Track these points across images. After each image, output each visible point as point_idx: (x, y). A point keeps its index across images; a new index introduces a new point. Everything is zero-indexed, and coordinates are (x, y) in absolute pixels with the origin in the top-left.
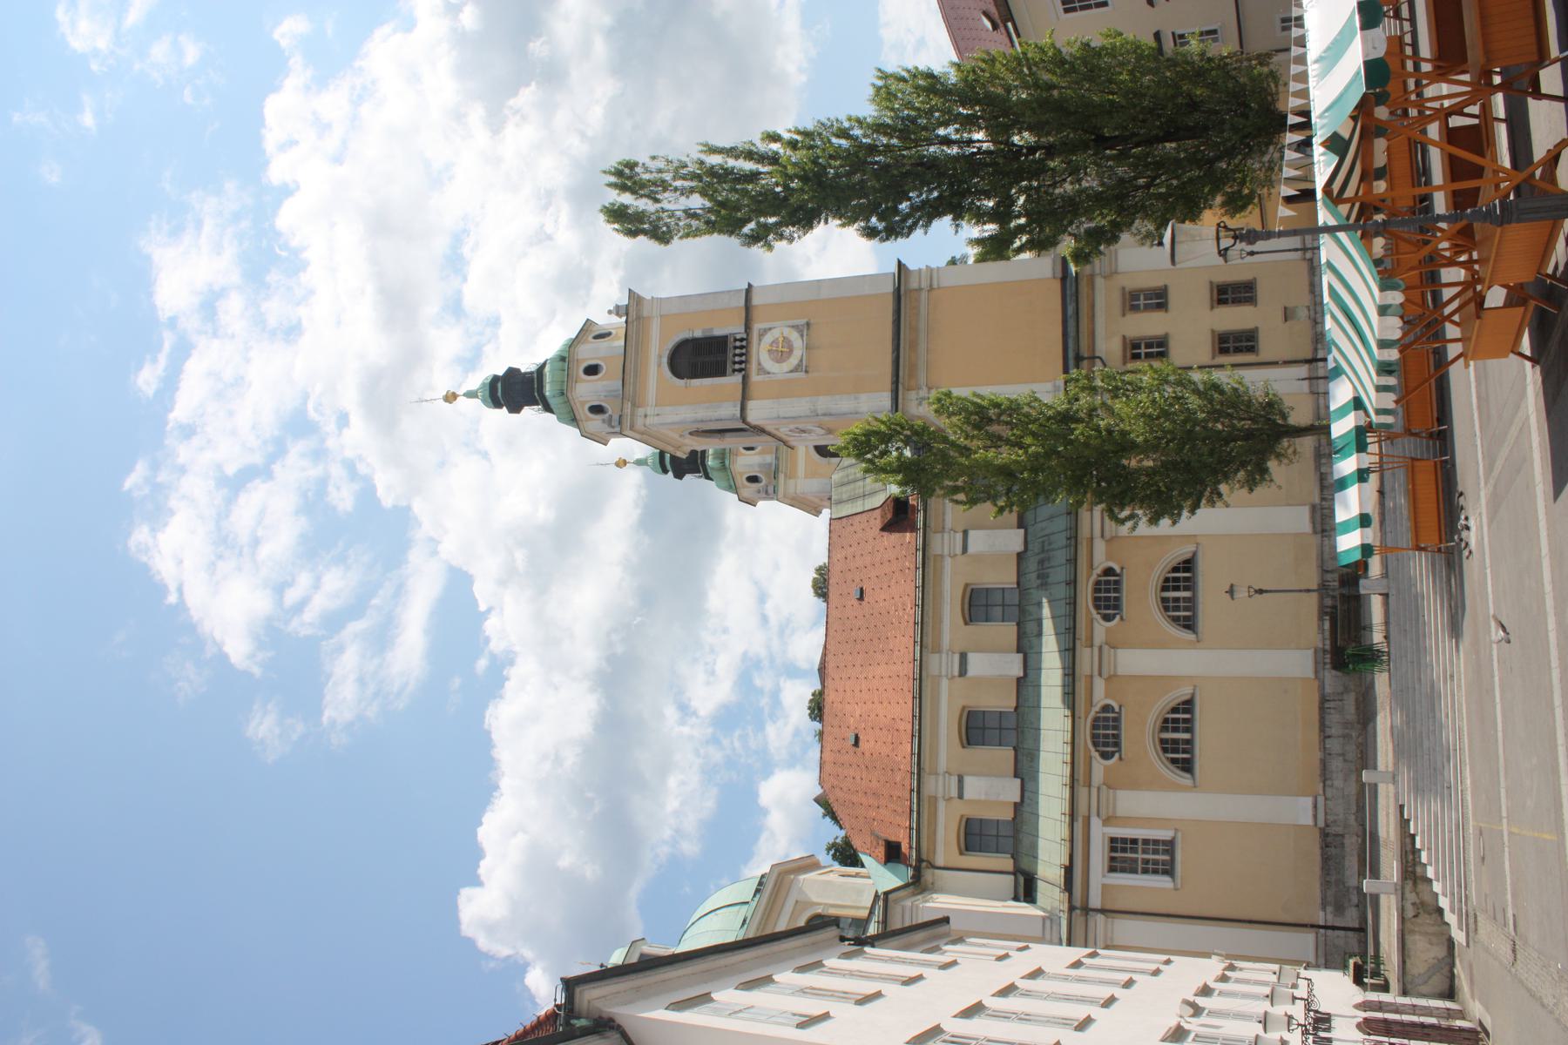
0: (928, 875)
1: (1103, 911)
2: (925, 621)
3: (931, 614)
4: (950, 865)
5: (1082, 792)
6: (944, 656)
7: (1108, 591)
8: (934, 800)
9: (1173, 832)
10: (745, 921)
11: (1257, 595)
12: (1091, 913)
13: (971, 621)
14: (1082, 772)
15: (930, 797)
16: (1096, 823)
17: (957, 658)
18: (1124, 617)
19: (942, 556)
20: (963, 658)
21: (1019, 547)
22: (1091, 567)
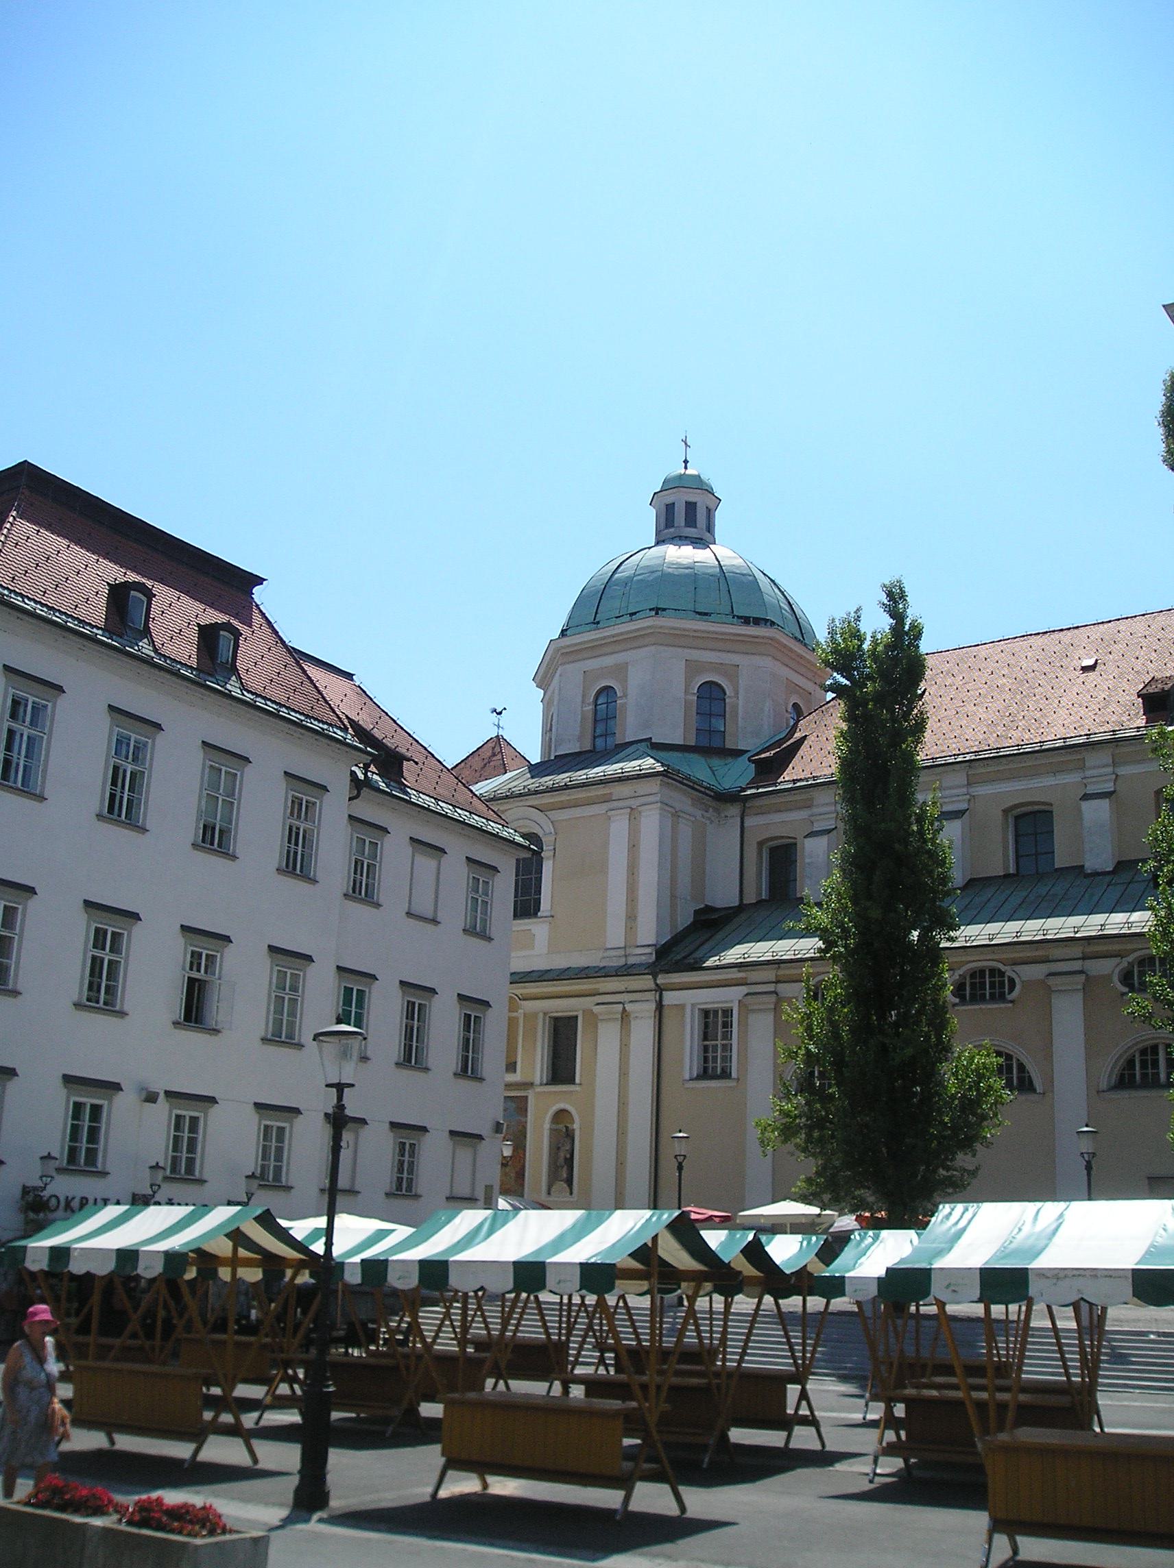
0: (734, 810)
1: (660, 1007)
2: (1001, 760)
3: (1011, 766)
4: (746, 835)
5: (769, 974)
6: (964, 790)
7: (992, 985)
8: (808, 805)
9: (736, 1077)
10: (706, 614)
11: (677, 1165)
12: (658, 994)
13: (1017, 818)
14: (787, 972)
15: (811, 799)
16: (736, 993)
17: (964, 806)
18: (956, 1008)
19: (1082, 768)
20: (958, 814)
21: (1091, 864)
22: (1015, 963)
